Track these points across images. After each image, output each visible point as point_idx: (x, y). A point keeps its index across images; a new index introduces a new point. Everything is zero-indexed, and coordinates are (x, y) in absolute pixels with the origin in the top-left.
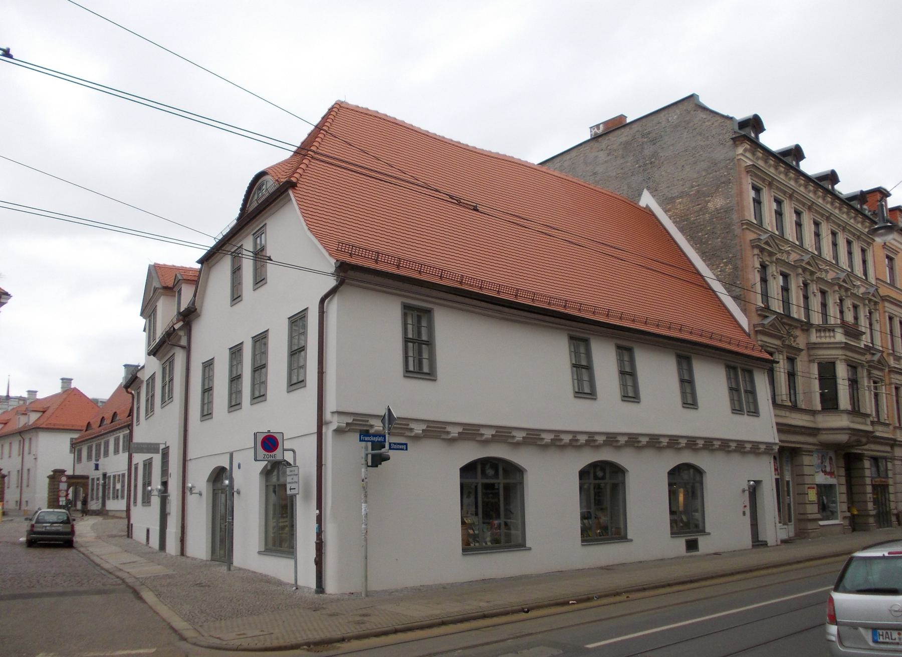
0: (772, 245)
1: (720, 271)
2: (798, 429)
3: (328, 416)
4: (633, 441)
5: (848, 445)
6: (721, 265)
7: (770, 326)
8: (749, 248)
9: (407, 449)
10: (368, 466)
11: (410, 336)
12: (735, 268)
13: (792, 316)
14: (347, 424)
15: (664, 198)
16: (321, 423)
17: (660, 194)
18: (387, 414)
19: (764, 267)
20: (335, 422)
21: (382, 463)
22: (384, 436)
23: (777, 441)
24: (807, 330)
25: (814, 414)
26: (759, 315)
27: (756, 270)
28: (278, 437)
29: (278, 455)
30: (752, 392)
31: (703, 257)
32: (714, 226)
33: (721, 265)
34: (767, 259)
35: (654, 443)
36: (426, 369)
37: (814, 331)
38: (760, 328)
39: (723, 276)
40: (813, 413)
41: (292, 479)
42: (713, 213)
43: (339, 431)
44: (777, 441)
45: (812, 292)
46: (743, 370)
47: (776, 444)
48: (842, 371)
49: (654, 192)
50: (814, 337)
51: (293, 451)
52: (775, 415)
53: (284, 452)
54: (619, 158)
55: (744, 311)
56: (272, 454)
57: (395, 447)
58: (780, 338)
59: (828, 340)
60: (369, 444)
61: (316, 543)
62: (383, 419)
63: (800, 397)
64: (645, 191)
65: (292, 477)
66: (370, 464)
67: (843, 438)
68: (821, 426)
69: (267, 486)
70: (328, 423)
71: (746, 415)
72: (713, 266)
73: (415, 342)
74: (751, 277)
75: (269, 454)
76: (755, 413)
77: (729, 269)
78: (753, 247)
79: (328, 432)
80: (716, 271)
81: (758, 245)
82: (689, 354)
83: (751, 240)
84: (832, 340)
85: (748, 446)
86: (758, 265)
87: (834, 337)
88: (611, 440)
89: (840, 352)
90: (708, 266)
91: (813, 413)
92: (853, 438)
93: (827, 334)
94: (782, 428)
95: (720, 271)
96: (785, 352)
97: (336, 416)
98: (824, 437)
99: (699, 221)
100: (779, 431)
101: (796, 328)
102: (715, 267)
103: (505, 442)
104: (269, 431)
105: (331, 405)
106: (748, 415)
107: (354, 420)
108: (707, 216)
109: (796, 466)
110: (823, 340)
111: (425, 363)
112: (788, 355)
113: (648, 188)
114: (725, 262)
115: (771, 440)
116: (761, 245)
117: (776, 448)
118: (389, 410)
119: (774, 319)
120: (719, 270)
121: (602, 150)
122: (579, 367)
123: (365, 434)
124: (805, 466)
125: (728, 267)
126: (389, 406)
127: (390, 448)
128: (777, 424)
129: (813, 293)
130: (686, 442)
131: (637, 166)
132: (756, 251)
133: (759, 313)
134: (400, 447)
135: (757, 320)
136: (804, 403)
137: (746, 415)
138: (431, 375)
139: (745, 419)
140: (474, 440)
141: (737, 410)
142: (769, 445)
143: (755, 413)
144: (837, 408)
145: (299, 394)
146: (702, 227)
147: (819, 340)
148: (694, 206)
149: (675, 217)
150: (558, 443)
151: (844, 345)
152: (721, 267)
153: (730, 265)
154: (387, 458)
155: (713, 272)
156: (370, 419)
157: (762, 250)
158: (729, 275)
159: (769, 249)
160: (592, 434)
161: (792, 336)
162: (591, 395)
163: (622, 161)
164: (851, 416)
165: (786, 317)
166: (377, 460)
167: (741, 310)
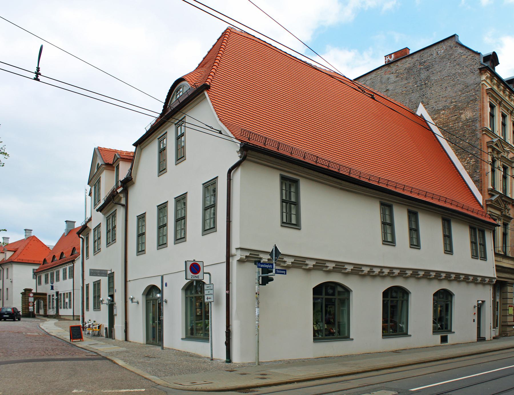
1: (467, 163)
3: (233, 251)
4: (415, 274)
6: (468, 159)
7: (495, 201)
8: (486, 147)
9: (286, 274)
10: (260, 285)
11: (284, 198)
12: (476, 161)
14: (246, 256)
15: (433, 110)
16: (229, 256)
17: (430, 107)
18: (274, 250)
19: (494, 161)
20: (238, 255)
21: (269, 282)
22: (272, 264)
23: (495, 277)
26: (489, 194)
28: (200, 264)
29: (200, 276)
30: (484, 245)
31: (456, 153)
32: (465, 131)
33: (468, 159)
34: (495, 155)
36: (294, 221)
38: (490, 203)
39: (468, 167)
41: (209, 292)
42: (464, 122)
43: (241, 261)
44: (495, 277)
46: (479, 230)
47: (494, 278)
49: (426, 105)
51: (209, 274)
52: (495, 261)
53: (204, 274)
54: (404, 80)
55: (481, 190)
56: (196, 275)
57: (279, 272)
60: (261, 269)
62: (271, 254)
64: (421, 104)
65: (208, 291)
66: (261, 283)
69: (186, 298)
70: (233, 256)
71: (479, 259)
72: (462, 159)
73: (288, 203)
74: (486, 167)
75: (195, 275)
77: (472, 162)
78: (488, 147)
79: (234, 262)
80: (464, 163)
81: (491, 145)
82: (450, 218)
83: (487, 142)
88: (403, 273)
90: (459, 159)
94: (499, 269)
95: (467, 163)
96: (502, 219)
97: (239, 251)
99: (455, 127)
100: (497, 271)
101: (509, 203)
102: (463, 160)
103: (340, 272)
104: (195, 260)
105: (235, 244)
106: (480, 259)
107: (250, 254)
109: (503, 292)
111: (293, 217)
112: (505, 221)
113: (423, 103)
114: (470, 157)
115: (492, 276)
116: (493, 146)
117: (495, 281)
118: (276, 247)
119: (498, 197)
120: (466, 162)
122: (385, 224)
123: (258, 262)
124: (508, 293)
125: (472, 161)
126: (275, 245)
127: (276, 273)
128: (496, 266)
130: (445, 275)
131: (416, 86)
132: (490, 150)
133: (490, 192)
134: (282, 272)
135: (488, 197)
136: (510, 253)
137: (479, 259)
138: (297, 226)
139: (479, 261)
140: (321, 270)
141: (475, 256)
145: (210, 236)
146: (457, 131)
148: (452, 117)
149: (439, 124)
150: (371, 274)
152: (468, 160)
153: (473, 159)
154: (272, 280)
155: (462, 164)
156: (260, 254)
157: (494, 149)
158: (472, 166)
159: (498, 149)
160: (391, 269)
161: (507, 209)
162: (393, 243)
163: (406, 82)
166: (266, 281)
167: (479, 190)
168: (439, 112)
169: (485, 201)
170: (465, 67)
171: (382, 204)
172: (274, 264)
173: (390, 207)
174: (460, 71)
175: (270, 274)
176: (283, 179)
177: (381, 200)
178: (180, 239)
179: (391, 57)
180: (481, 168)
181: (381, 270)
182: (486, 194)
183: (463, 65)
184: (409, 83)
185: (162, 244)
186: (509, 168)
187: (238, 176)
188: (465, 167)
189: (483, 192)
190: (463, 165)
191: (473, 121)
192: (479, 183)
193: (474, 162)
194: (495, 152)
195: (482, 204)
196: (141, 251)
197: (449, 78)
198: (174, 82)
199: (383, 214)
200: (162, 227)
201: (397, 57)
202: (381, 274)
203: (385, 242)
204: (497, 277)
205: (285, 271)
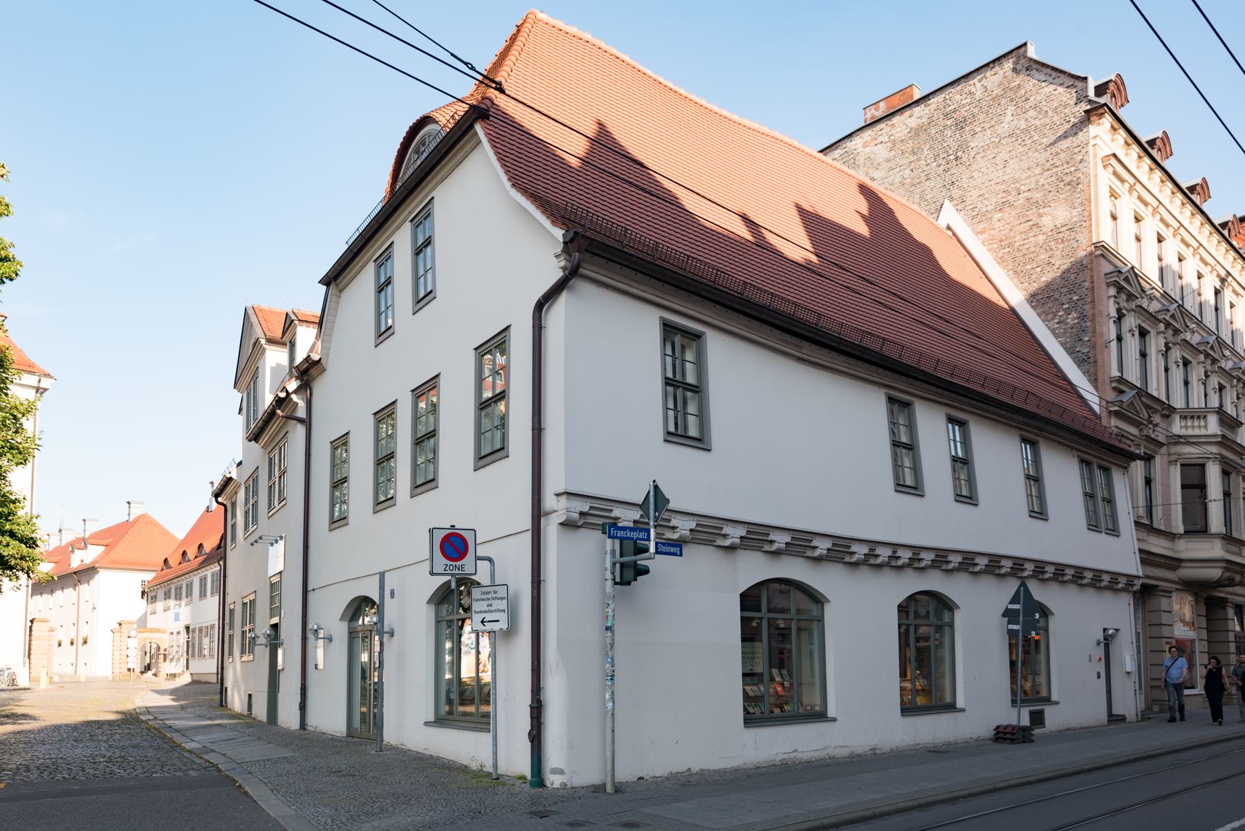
0: (1132, 284)
1: (1058, 323)
2: (1157, 559)
3: (549, 502)
4: (968, 563)
5: (1218, 584)
6: (1060, 314)
7: (1128, 406)
8: (1104, 286)
9: (681, 555)
10: (616, 583)
11: (670, 375)
12: (1083, 317)
13: (1149, 391)
14: (582, 514)
15: (975, 213)
17: (970, 207)
18: (652, 493)
19: (1120, 317)
21: (638, 578)
24: (1167, 417)
25: (1174, 538)
26: (1114, 388)
27: (1111, 321)
28: (468, 536)
29: (468, 562)
30: (1110, 501)
31: (1032, 302)
32: (1051, 253)
33: (1060, 314)
34: (1124, 304)
35: (994, 566)
36: (693, 431)
37: (1178, 417)
38: (1117, 408)
39: (1061, 331)
40: (1172, 536)
41: (491, 605)
42: (1050, 233)
43: (567, 525)
44: (1141, 574)
45: (1174, 361)
46: (1100, 467)
47: (1138, 577)
48: (1213, 474)
49: (960, 204)
50: (1177, 427)
51: (490, 560)
53: (478, 561)
54: (907, 155)
55: (1094, 381)
56: (457, 564)
57: (664, 549)
58: (1137, 424)
59: (1197, 432)
60: (617, 542)
61: (532, 708)
62: (644, 506)
63: (1158, 512)
64: (947, 202)
65: (489, 602)
66: (618, 580)
67: (1215, 573)
68: (1183, 556)
69: (438, 622)
70: (547, 514)
71: (1103, 533)
72: (1047, 315)
73: (679, 387)
74: (1105, 330)
75: (454, 563)
76: (1114, 531)
77: (1072, 319)
78: (1108, 285)
79: (551, 530)
80: (1052, 322)
81: (1116, 281)
82: (1037, 438)
83: (1105, 274)
84: (1203, 432)
85: (1106, 578)
86: (1114, 313)
87: (1206, 427)
88: (941, 559)
89: (1214, 449)
90: (1039, 316)
91: (1172, 536)
92: (1227, 574)
93: (1196, 423)
95: (1058, 323)
96: (1143, 446)
97: (563, 499)
98: (1188, 572)
99: (1028, 246)
101: (1156, 411)
102: (1050, 316)
103: (801, 555)
104: (454, 526)
105: (554, 481)
106: (1106, 533)
107: (591, 508)
108: (1041, 238)
109: (1149, 611)
110: (1190, 432)
111: (692, 421)
112: (1146, 451)
113: (951, 199)
114: (1067, 308)
115: (1134, 572)
116: (1121, 282)
117: (1138, 583)
118: (656, 487)
119: (1134, 396)
120: (1057, 320)
121: (882, 143)
122: (899, 446)
123: (611, 528)
124: (1163, 614)
125: (1070, 317)
126: (654, 481)
127: (657, 552)
129: (1176, 362)
130: (1033, 568)
131: (935, 164)
132: (1112, 291)
133: (1114, 385)
134: (672, 550)
135: (1111, 396)
136: (1162, 523)
137: (1103, 533)
138: (701, 442)
139: (1103, 538)
140: (759, 549)
141: (1094, 526)
142: (1131, 578)
143: (1114, 531)
144: (1206, 531)
145: (495, 470)
146: (1032, 256)
147: (1183, 432)
148: (1020, 224)
149: (991, 242)
150: (872, 561)
151: (1220, 440)
152: (1061, 316)
153: (1073, 313)
154: (645, 571)
155: (1046, 325)
156: (614, 509)
157: (1120, 289)
158: (1072, 328)
159: (1130, 290)
160: (916, 549)
161: (1151, 423)
162: (916, 489)
163: (912, 158)
164: (1224, 542)
165: (1142, 393)
167: (1089, 380)
168: (989, 216)
170: (1050, 112)
171: (891, 400)
173: (907, 405)
174: (1038, 123)
178: (424, 483)
179: (876, 110)
180: (1094, 332)
183: (1045, 109)
184: (919, 160)
185: (383, 502)
186: (1153, 332)
187: (557, 314)
188: (1053, 331)
189: (1099, 384)
190: (1049, 328)
191: (1070, 229)
192: (1088, 362)
193: (1074, 319)
194: (1124, 297)
196: (338, 522)
197: (1013, 139)
198: (407, 129)
200: (384, 460)
201: (894, 107)
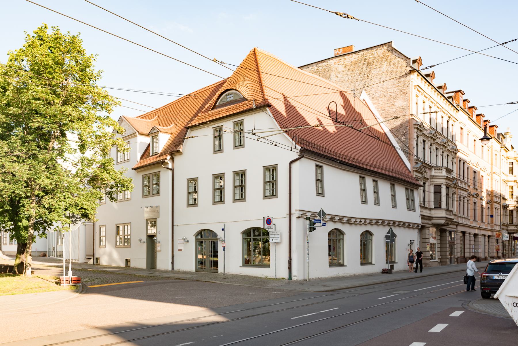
3: (293, 211)
8: (413, 128)
12: (406, 138)
15: (373, 97)
16: (290, 214)
20: (298, 214)
22: (321, 220)
23: (421, 223)
25: (431, 210)
27: (415, 140)
30: (413, 200)
35: (383, 223)
38: (416, 169)
40: (430, 209)
44: (421, 223)
46: (411, 190)
47: (420, 224)
52: (421, 211)
55: (409, 160)
67: (443, 222)
68: (433, 216)
74: (413, 143)
76: (414, 210)
77: (403, 138)
78: (414, 128)
82: (395, 183)
86: (416, 137)
89: (444, 180)
91: (430, 209)
92: (447, 222)
94: (423, 217)
100: (422, 218)
108: (394, 110)
128: (421, 215)
132: (416, 130)
133: (415, 161)
135: (414, 164)
139: (411, 212)
141: (408, 209)
143: (414, 210)
144: (441, 208)
157: (418, 129)
160: (365, 219)
164: (446, 211)
166: (312, 229)
167: (408, 159)
168: (377, 99)
169: (412, 167)
170: (398, 67)
172: (321, 220)
173: (363, 178)
174: (394, 70)
175: (315, 225)
176: (360, 177)
177: (405, 186)
180: (410, 144)
181: (356, 220)
182: (413, 162)
183: (397, 66)
186: (427, 141)
188: (397, 142)
189: (411, 161)
190: (396, 140)
192: (408, 153)
193: (404, 138)
194: (419, 131)
195: (410, 170)
197: (386, 74)
199: (407, 194)
202: (355, 223)
203: (318, 194)
204: (422, 223)
205: (326, 224)
